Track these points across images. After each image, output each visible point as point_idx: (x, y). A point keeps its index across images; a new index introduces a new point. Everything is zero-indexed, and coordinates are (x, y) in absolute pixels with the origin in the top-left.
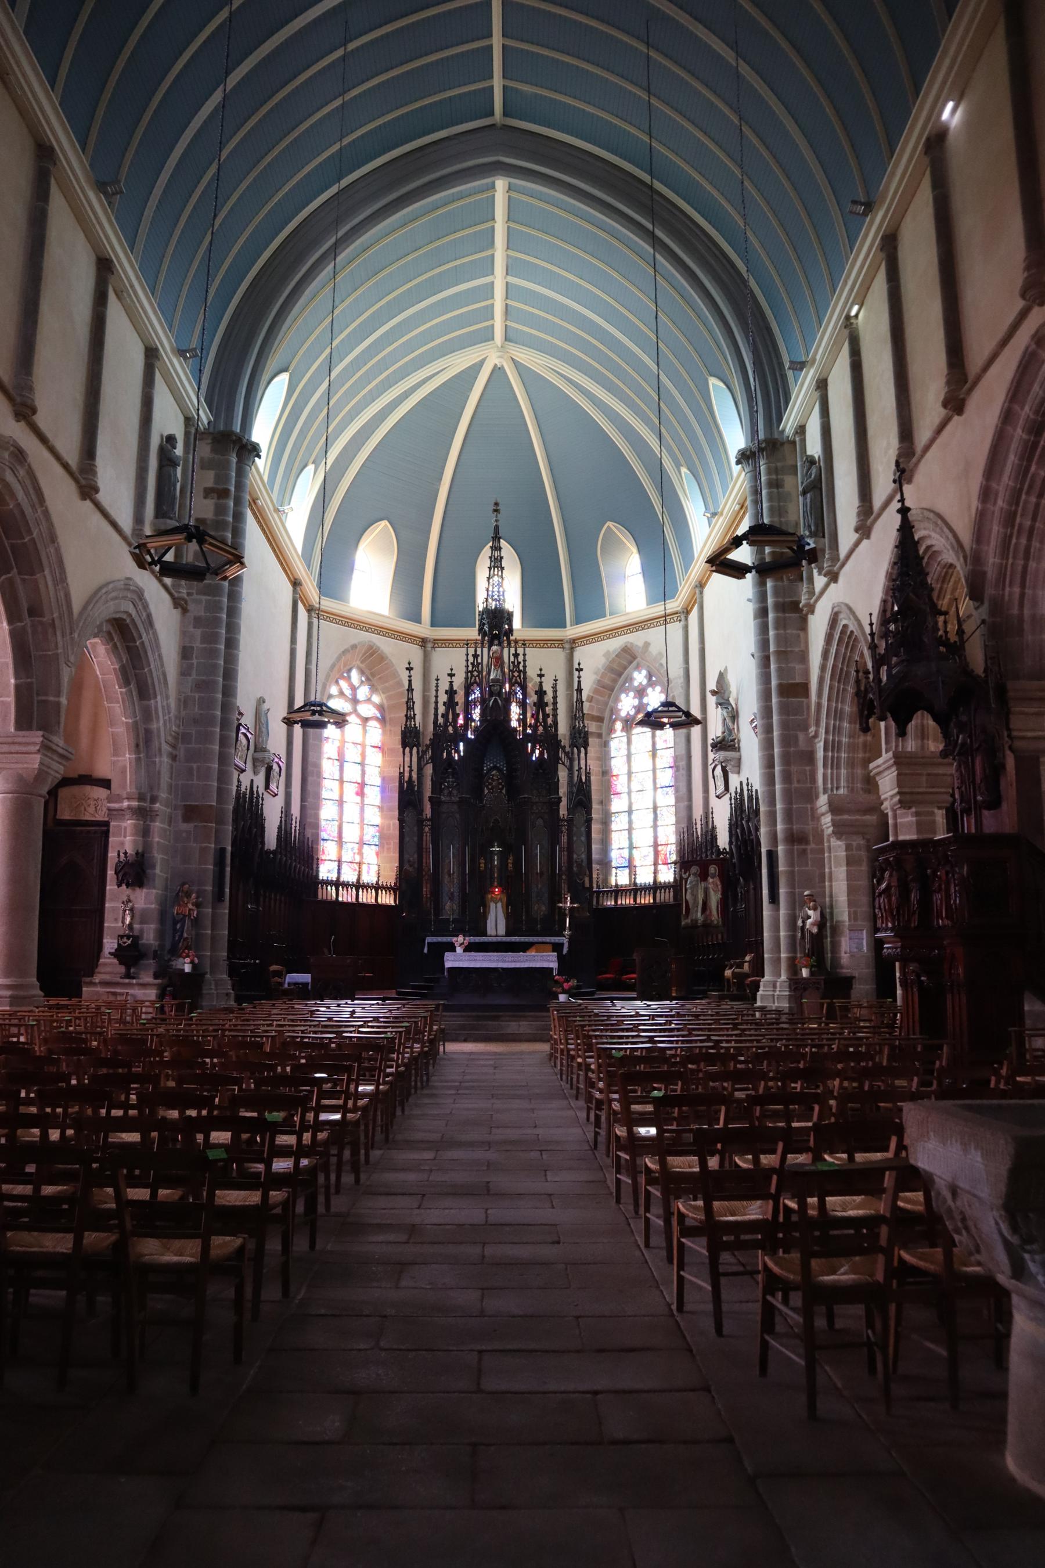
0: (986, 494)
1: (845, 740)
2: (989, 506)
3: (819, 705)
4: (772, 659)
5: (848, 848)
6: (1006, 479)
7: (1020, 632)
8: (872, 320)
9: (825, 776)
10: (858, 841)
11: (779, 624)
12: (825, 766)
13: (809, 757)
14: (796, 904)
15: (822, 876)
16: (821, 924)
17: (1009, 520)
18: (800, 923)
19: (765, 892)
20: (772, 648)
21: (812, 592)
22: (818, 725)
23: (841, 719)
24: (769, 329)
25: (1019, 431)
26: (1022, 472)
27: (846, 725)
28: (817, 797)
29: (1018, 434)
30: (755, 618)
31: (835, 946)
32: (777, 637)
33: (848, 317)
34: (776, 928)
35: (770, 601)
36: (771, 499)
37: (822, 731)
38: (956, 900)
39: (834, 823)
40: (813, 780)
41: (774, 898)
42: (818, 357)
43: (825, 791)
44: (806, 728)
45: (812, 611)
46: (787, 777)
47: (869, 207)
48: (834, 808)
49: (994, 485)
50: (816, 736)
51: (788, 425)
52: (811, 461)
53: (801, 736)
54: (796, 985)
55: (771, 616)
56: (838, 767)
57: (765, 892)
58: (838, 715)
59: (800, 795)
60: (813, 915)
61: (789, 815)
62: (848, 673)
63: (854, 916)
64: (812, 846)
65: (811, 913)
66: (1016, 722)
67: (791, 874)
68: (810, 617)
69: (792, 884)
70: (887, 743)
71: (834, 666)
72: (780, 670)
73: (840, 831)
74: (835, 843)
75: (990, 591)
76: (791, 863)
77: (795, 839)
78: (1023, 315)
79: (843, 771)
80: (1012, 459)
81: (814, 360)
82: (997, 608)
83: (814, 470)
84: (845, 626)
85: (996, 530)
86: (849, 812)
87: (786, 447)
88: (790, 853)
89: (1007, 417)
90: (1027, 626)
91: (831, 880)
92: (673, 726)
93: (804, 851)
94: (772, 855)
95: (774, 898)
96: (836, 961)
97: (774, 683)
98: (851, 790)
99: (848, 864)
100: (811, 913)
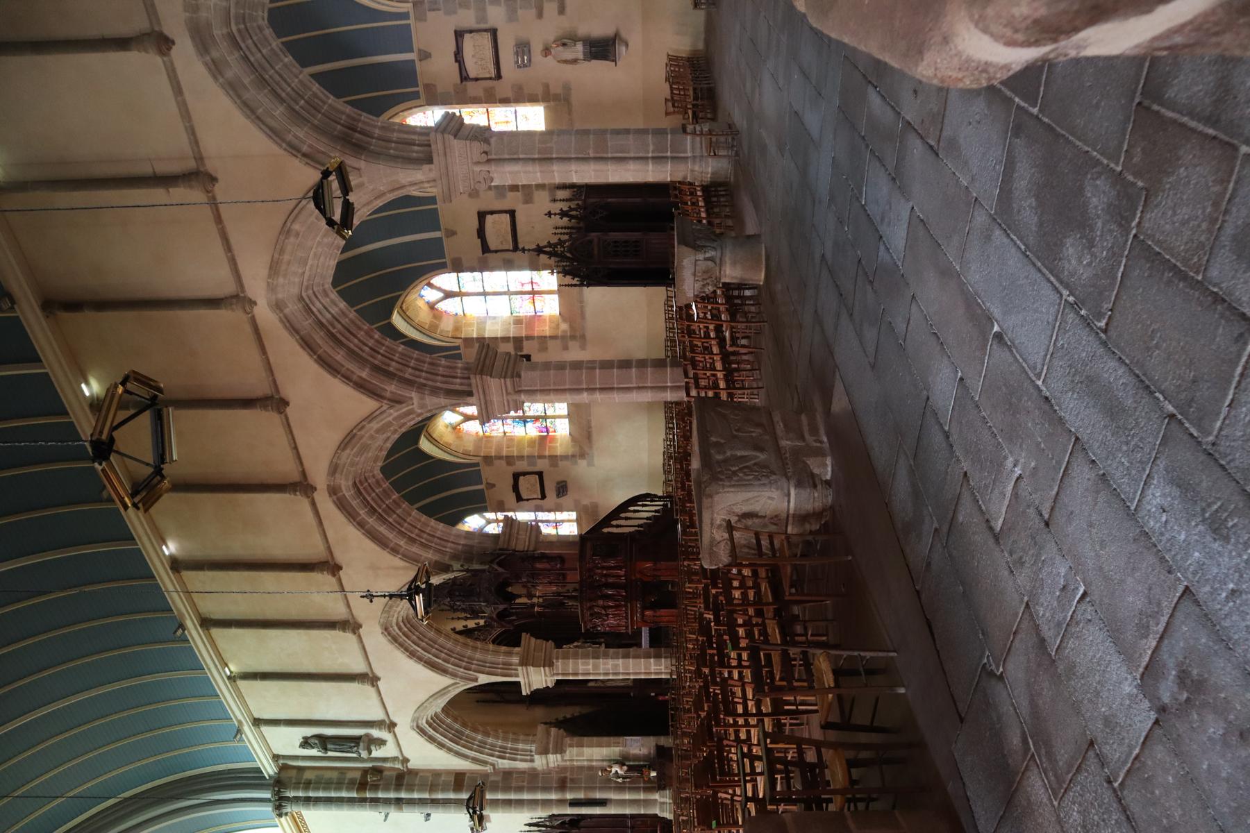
0: (395, 551)
1: (500, 743)
2: (402, 550)
3: (475, 760)
4: (434, 797)
5: (571, 746)
6: (390, 535)
7: (472, 547)
8: (246, 649)
9: (522, 760)
10: (568, 740)
11: (410, 789)
12: (515, 760)
13: (507, 774)
14: (608, 784)
15: (590, 768)
16: (622, 764)
17: (412, 540)
18: (620, 780)
19: (597, 811)
20: (426, 796)
21: (395, 759)
22: (485, 763)
23: (485, 743)
24: (190, 778)
25: (370, 520)
26: (391, 526)
27: (490, 740)
28: (534, 769)
29: (371, 521)
30: (401, 809)
31: (636, 758)
32: (421, 790)
33: (229, 678)
34: (622, 803)
35: (392, 795)
36: (317, 789)
37: (491, 759)
38: (612, 563)
39: (555, 752)
40: (522, 772)
41: (602, 803)
42: (240, 717)
43: (532, 761)
44: (486, 775)
45: (406, 760)
46: (520, 789)
47: (182, 626)
48: (544, 751)
49: (392, 545)
50: (493, 765)
51: (269, 769)
52: (306, 743)
53: (492, 778)
54: (660, 785)
55: (403, 795)
56: (517, 750)
57: (597, 811)
58: (482, 745)
59: (533, 780)
60: (615, 769)
61: (546, 789)
62: (457, 731)
63: (617, 744)
64: (568, 774)
65: (613, 770)
66: (520, 547)
67: (588, 789)
68: (410, 765)
69: (593, 789)
70: (510, 676)
71: (451, 740)
72: (444, 790)
73: (559, 749)
74: (567, 757)
75: (446, 560)
76: (579, 788)
77: (562, 785)
78: (313, 504)
79: (521, 746)
80: (382, 529)
81: (240, 722)
82: (455, 557)
83: (312, 741)
84: (427, 722)
85: (415, 549)
86: (548, 743)
87: (284, 775)
88: (572, 789)
89: (361, 525)
90: (470, 542)
91: (592, 760)
92: (482, 809)
93: (572, 780)
94: (575, 803)
95: (602, 803)
96: (645, 758)
97: (452, 796)
98: (533, 742)
99: (582, 746)
100: (613, 770)
